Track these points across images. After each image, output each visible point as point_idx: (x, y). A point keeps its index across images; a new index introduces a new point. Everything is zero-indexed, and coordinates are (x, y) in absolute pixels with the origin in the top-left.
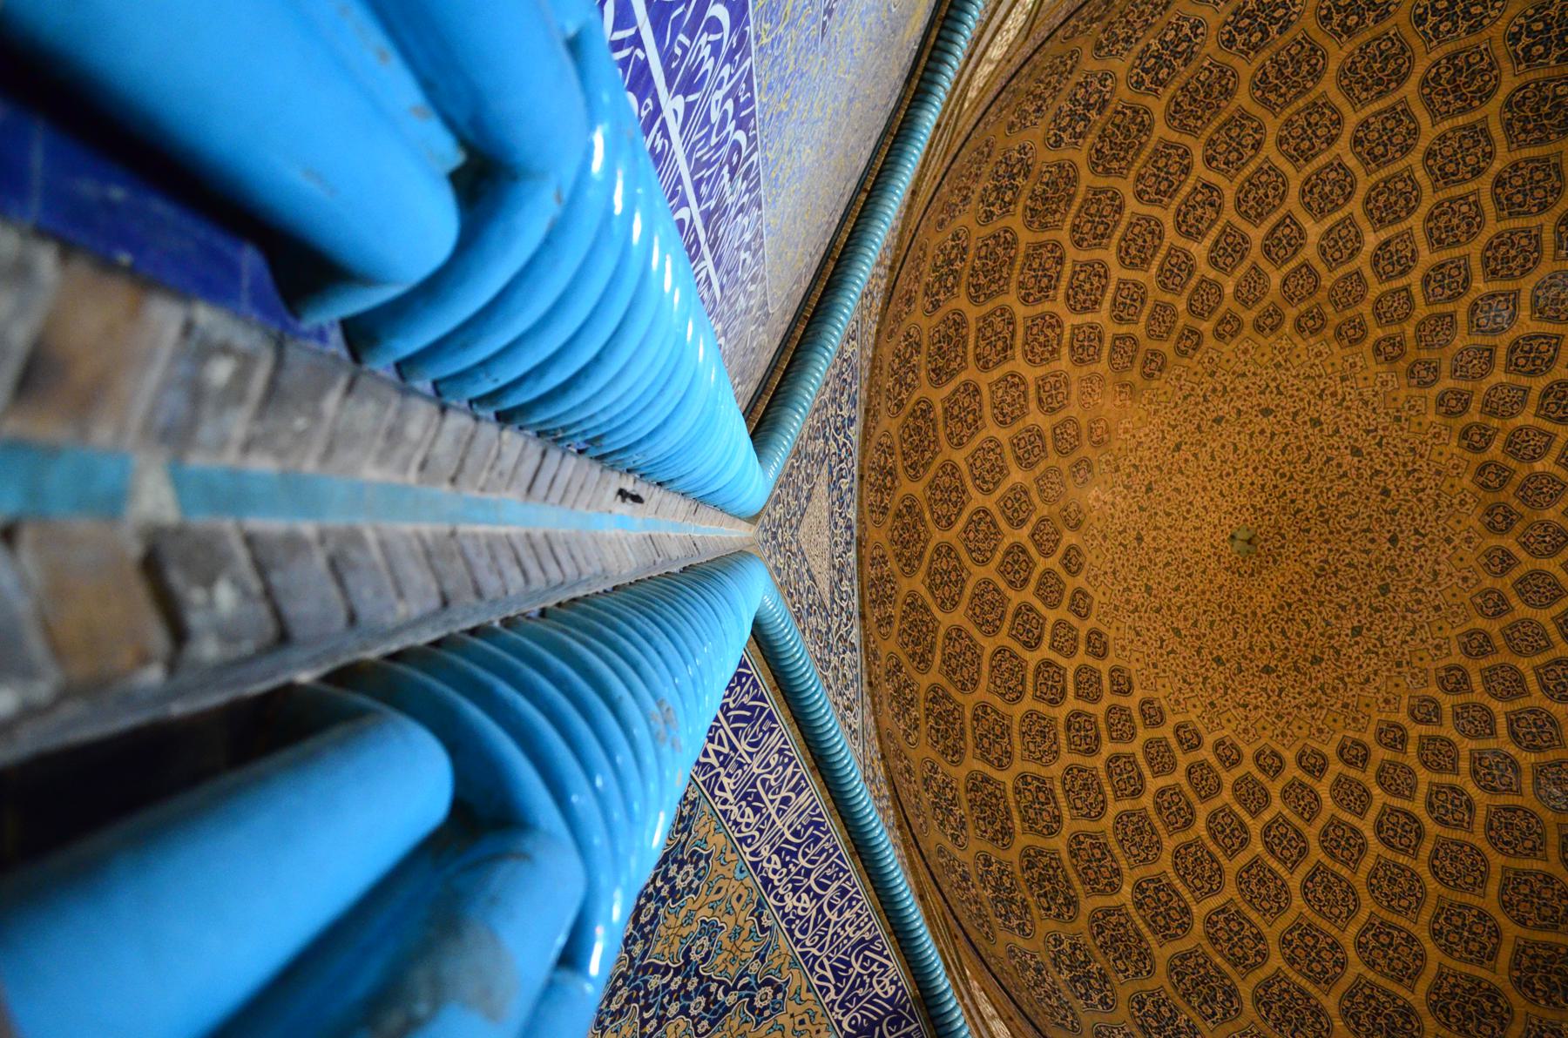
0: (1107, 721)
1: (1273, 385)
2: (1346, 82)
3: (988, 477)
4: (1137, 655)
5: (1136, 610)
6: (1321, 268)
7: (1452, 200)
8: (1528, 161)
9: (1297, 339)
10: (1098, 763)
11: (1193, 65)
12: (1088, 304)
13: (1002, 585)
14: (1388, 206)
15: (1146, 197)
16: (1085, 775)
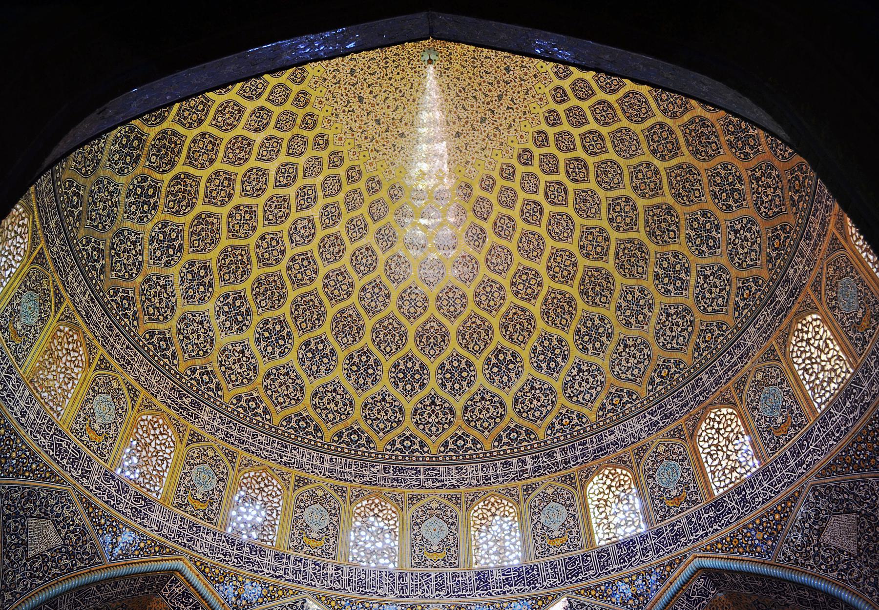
0: (566, 152)
1: (347, 109)
2: (218, 236)
3: (471, 267)
4: (522, 126)
5: (497, 128)
6: (285, 145)
7: (220, 128)
8: (184, 125)
9: (320, 120)
10: (591, 161)
11: (267, 315)
12: (370, 253)
13: (517, 236)
14: (241, 149)
15: (315, 267)
16: (599, 172)
